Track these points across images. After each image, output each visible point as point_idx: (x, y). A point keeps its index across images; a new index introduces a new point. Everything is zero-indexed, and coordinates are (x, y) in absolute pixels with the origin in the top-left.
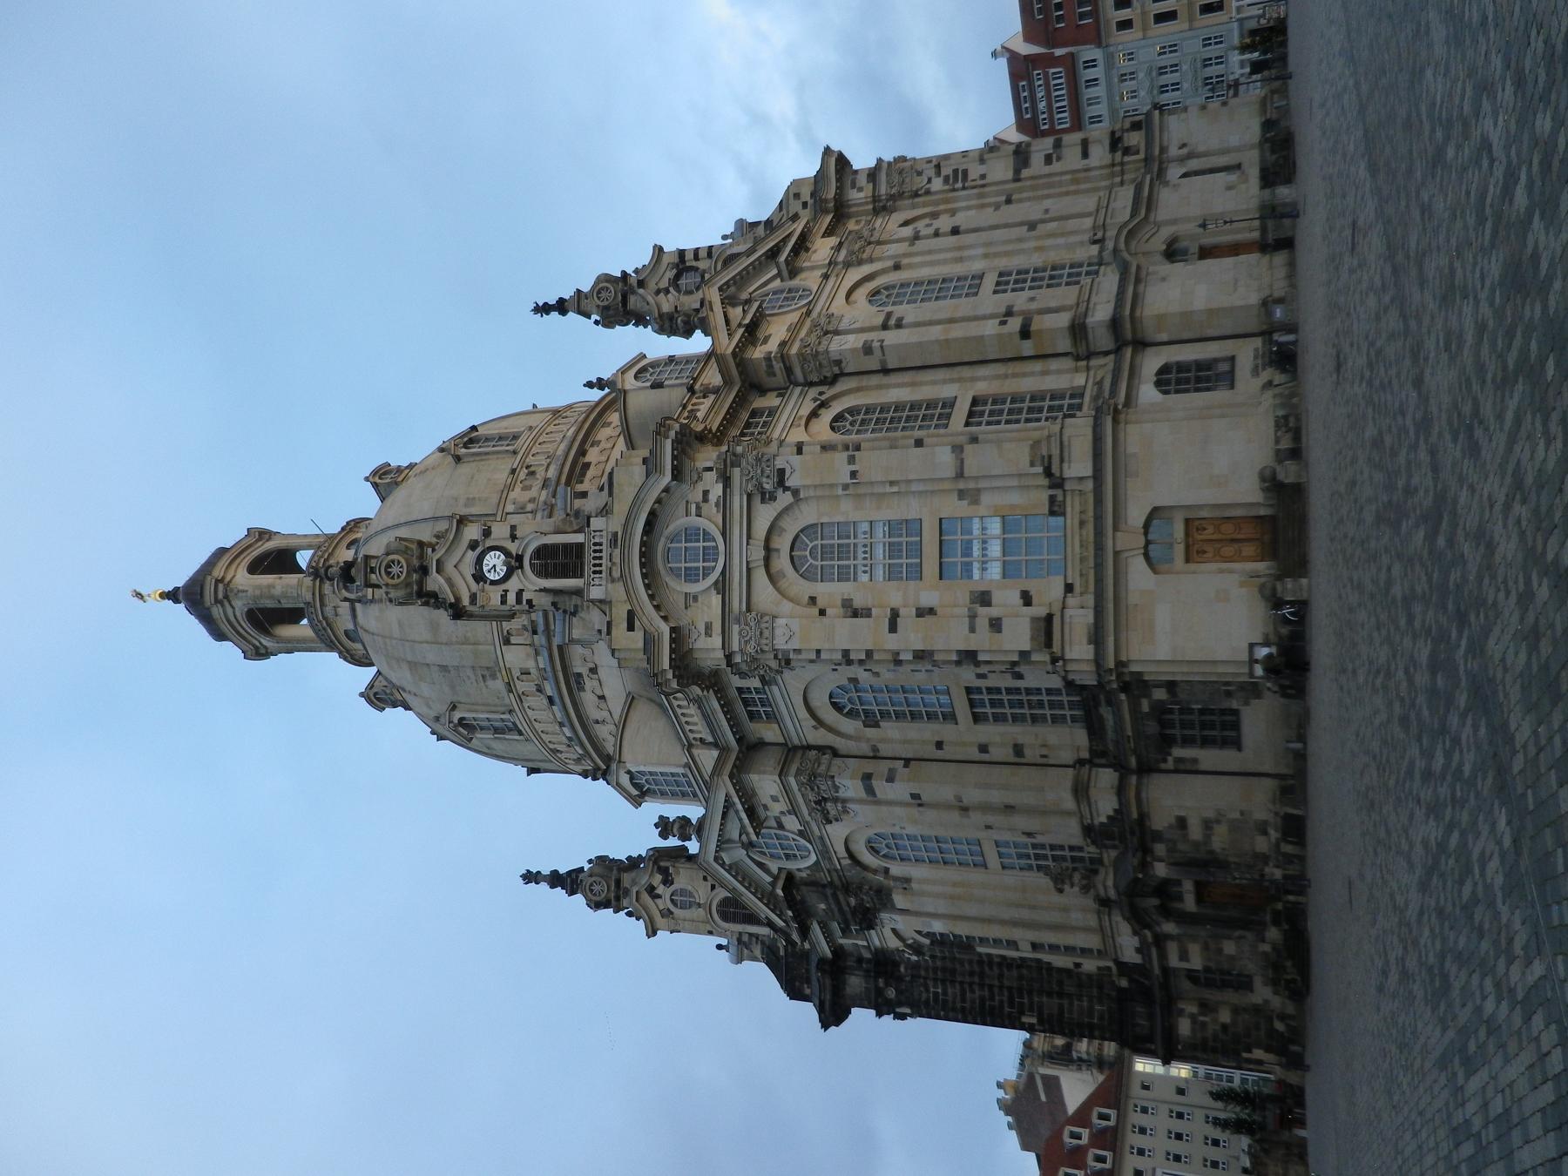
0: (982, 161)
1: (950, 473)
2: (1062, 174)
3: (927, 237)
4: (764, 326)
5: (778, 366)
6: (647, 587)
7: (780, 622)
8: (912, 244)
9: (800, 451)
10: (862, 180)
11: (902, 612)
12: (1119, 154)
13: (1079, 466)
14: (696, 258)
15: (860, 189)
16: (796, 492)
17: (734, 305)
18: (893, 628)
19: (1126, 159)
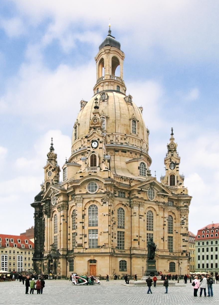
0: (185, 227)
1: (104, 231)
2: (180, 242)
3: (164, 220)
4: (143, 192)
5: (133, 196)
6: (86, 180)
7: (81, 204)
8: (162, 217)
9: (109, 206)
10: (185, 204)
11: (83, 224)
12: (182, 252)
13: (103, 250)
14: (177, 168)
15: (183, 204)
16: (102, 205)
17: (150, 185)
18: (80, 223)
19: (181, 253)
